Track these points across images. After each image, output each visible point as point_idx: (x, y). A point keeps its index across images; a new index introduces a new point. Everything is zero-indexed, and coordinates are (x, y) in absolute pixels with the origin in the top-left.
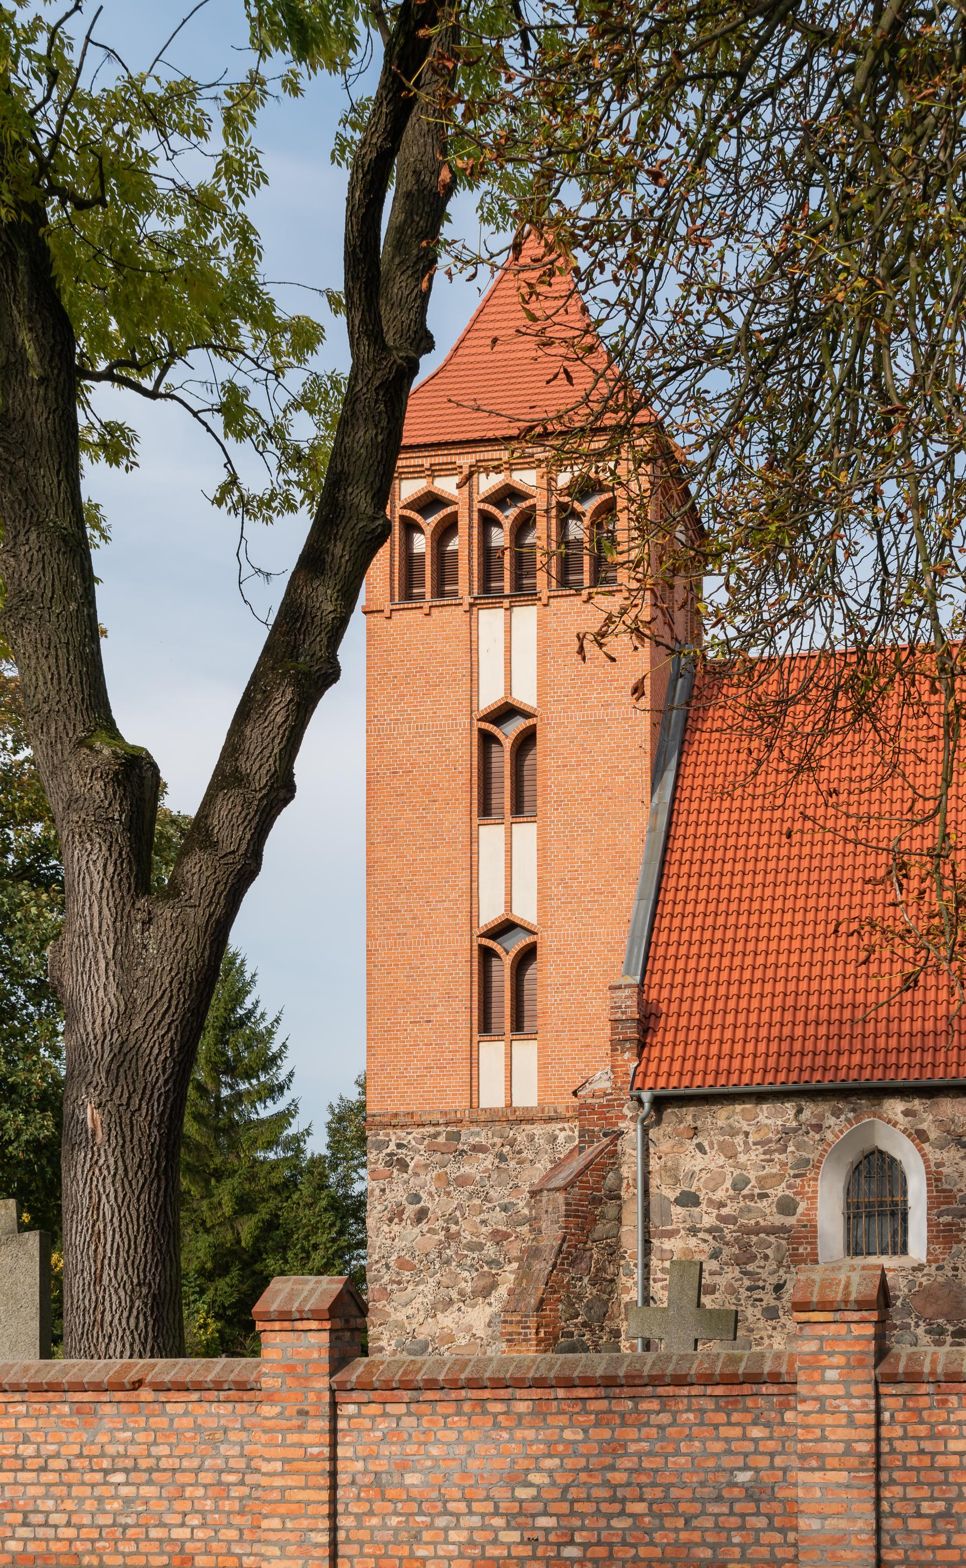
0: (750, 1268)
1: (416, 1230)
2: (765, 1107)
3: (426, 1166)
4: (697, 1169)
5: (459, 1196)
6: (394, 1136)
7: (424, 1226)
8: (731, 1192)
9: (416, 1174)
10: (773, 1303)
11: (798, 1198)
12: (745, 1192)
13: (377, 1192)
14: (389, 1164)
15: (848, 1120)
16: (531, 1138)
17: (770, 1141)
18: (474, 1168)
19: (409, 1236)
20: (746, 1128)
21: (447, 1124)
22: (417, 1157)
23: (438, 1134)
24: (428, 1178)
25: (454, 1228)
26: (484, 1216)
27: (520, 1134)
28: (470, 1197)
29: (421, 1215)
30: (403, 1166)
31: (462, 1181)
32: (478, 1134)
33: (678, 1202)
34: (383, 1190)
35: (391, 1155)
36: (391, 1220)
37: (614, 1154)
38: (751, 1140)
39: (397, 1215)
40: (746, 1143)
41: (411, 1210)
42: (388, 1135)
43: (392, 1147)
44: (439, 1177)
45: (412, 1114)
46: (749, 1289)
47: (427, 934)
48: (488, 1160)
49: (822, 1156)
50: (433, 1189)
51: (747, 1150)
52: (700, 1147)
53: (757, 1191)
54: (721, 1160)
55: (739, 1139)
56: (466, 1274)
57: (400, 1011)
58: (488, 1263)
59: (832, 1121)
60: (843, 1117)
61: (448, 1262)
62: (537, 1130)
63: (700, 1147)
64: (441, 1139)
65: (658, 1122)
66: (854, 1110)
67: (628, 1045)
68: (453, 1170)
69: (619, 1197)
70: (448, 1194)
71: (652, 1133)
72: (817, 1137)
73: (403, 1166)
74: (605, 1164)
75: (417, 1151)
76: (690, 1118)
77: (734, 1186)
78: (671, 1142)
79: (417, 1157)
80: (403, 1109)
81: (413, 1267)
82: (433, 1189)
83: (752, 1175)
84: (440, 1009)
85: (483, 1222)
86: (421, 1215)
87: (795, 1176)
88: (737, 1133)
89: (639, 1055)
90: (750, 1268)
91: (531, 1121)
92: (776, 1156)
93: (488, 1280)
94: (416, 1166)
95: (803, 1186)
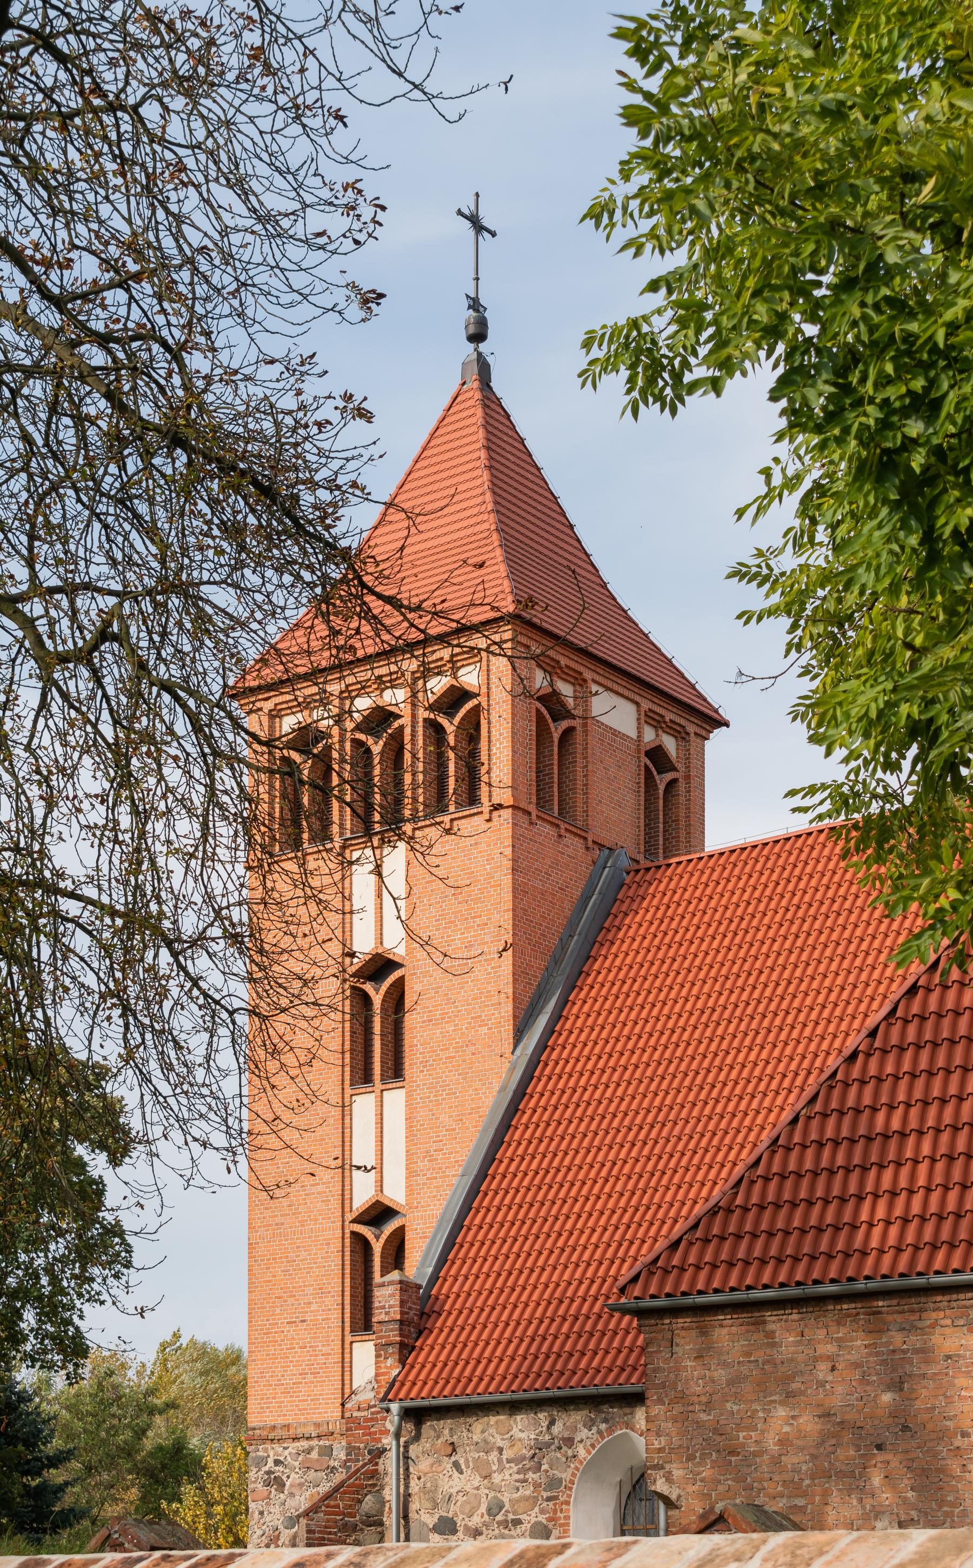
2: (518, 1418)
3: (301, 1485)
4: (454, 1491)
6: (273, 1451)
8: (486, 1517)
11: (550, 1525)
12: (499, 1517)
15: (600, 1432)
17: (523, 1458)
20: (500, 1443)
21: (319, 1437)
22: (293, 1475)
23: (309, 1451)
33: (436, 1529)
34: (261, 1513)
35: (269, 1473)
37: (374, 1474)
38: (504, 1457)
40: (500, 1460)
42: (266, 1450)
43: (270, 1463)
45: (287, 1427)
47: (303, 1223)
49: (574, 1475)
51: (501, 1470)
52: (456, 1465)
53: (511, 1516)
54: (477, 1481)
55: (494, 1456)
59: (583, 1433)
60: (594, 1429)
63: (456, 1465)
64: (314, 1455)
65: (417, 1437)
66: (606, 1421)
67: (390, 1350)
69: (381, 1524)
71: (414, 1450)
72: (570, 1453)
73: (281, 1485)
74: (361, 1486)
76: (446, 1432)
77: (489, 1510)
78: (430, 1460)
80: (280, 1421)
83: (505, 1498)
84: (314, 1307)
87: (549, 1499)
88: (492, 1449)
89: (403, 1362)
92: (530, 1475)
95: (555, 1511)
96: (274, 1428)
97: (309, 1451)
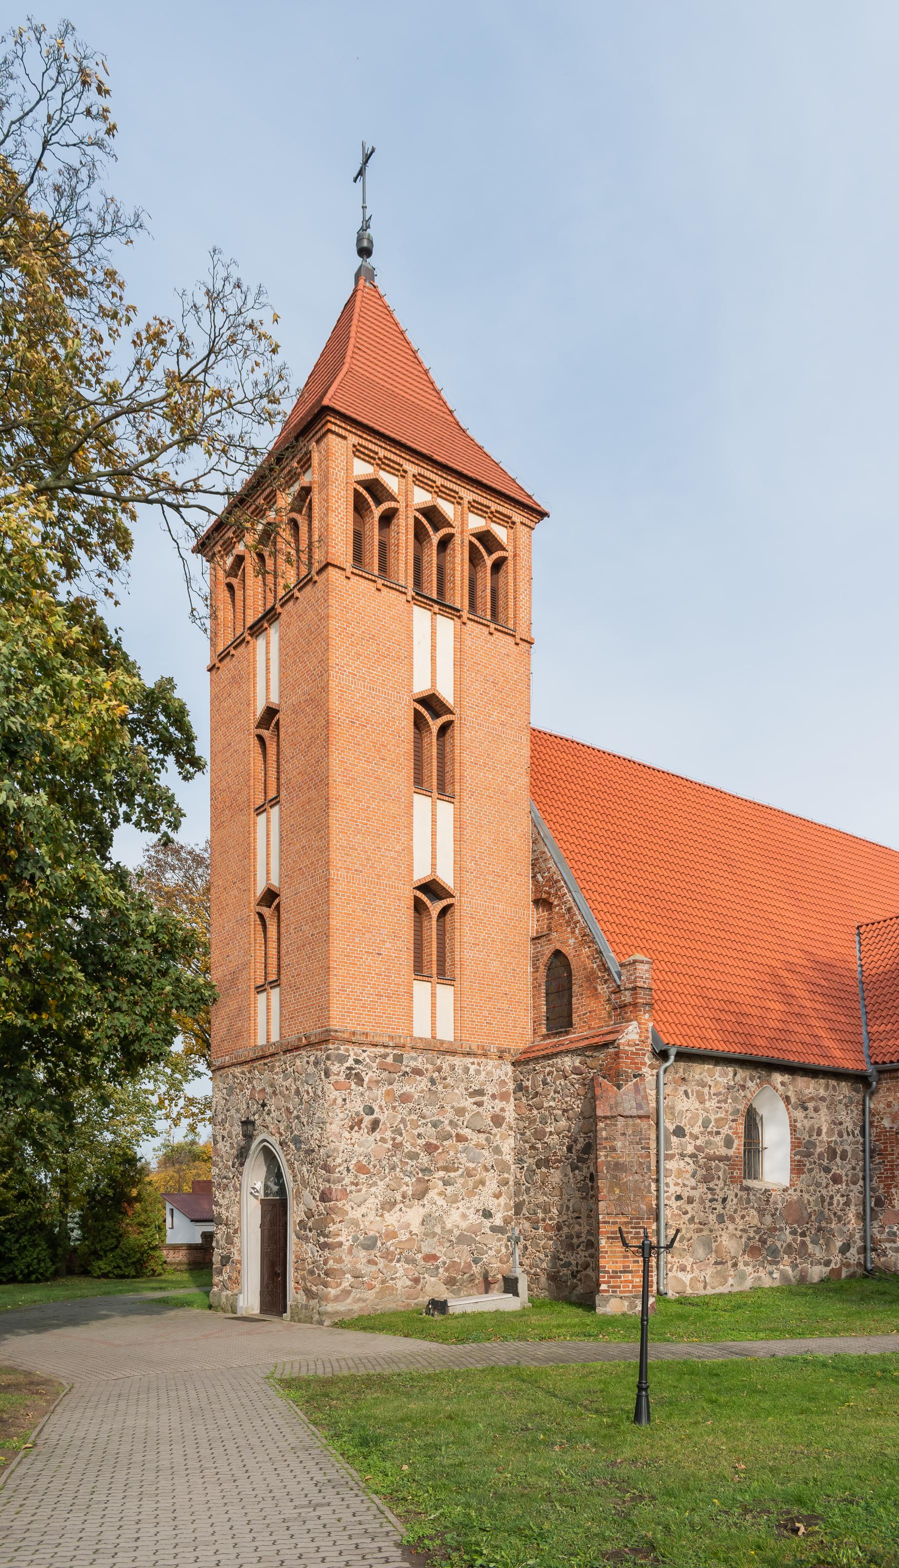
0: (711, 1185)
1: (371, 1138)
3: (377, 1082)
5: (403, 1110)
6: (353, 1052)
7: (377, 1135)
9: (369, 1088)
10: (722, 1211)
13: (339, 1101)
14: (348, 1077)
16: (453, 1068)
18: (416, 1087)
19: (365, 1144)
21: (394, 1047)
22: (370, 1073)
23: (385, 1056)
24: (379, 1092)
25: (399, 1139)
26: (421, 1130)
27: (446, 1062)
28: (410, 1113)
29: (375, 1125)
30: (360, 1081)
31: (405, 1098)
32: (415, 1059)
34: (344, 1100)
35: (350, 1069)
36: (352, 1128)
39: (356, 1124)
41: (367, 1119)
42: (347, 1050)
43: (350, 1062)
44: (388, 1093)
45: (366, 1034)
46: (711, 1201)
48: (423, 1083)
50: (383, 1103)
56: (407, 1179)
57: (357, 940)
58: (422, 1170)
61: (393, 1168)
62: (457, 1061)
64: (390, 1059)
68: (399, 1088)
70: (394, 1108)
73: (360, 1081)
75: (370, 1068)
79: (370, 1073)
81: (368, 1172)
82: (383, 1103)
85: (419, 1135)
86: (375, 1125)
90: (711, 1185)
91: (453, 1053)
93: (421, 1187)
94: (370, 1082)
96: (354, 1033)
97: (385, 1056)
